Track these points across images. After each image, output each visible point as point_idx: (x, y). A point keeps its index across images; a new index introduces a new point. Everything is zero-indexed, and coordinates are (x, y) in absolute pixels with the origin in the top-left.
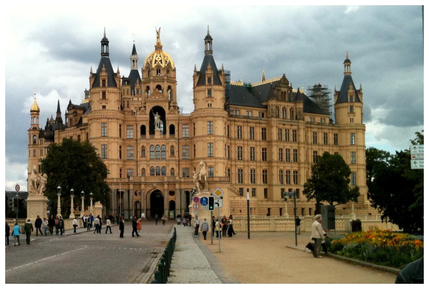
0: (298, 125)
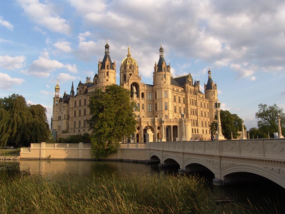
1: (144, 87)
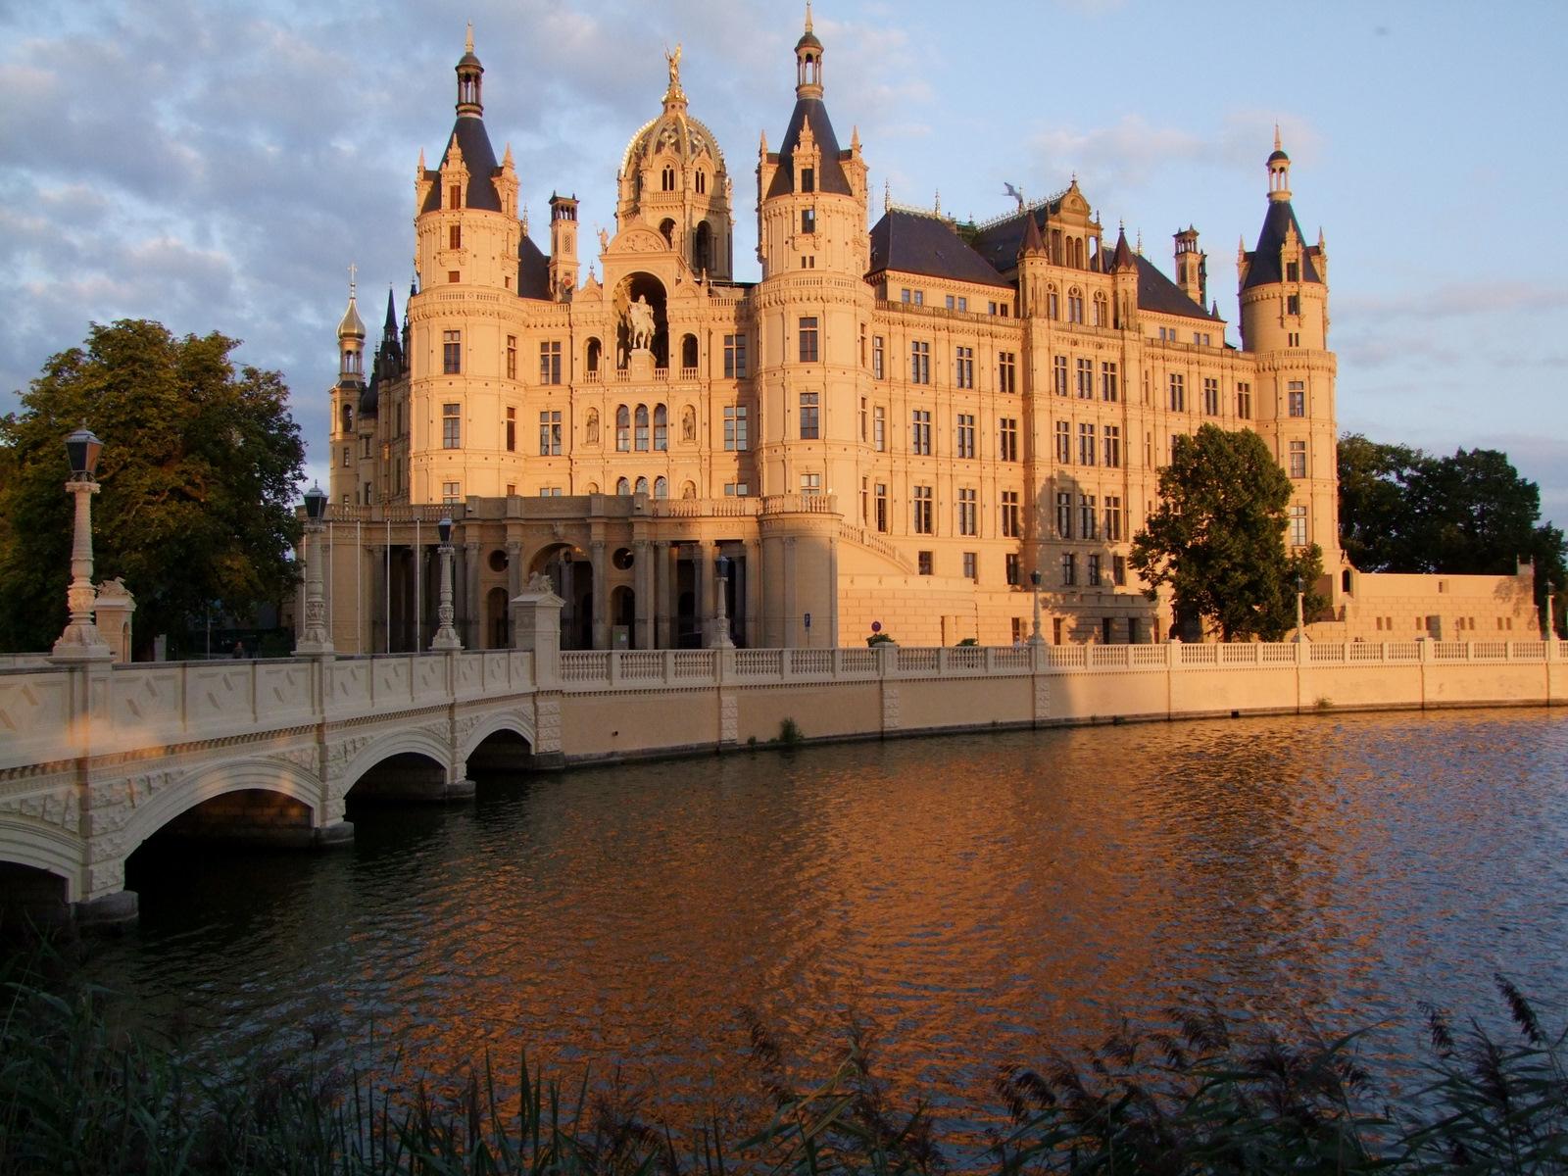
0: (1123, 349)
1: (694, 303)
